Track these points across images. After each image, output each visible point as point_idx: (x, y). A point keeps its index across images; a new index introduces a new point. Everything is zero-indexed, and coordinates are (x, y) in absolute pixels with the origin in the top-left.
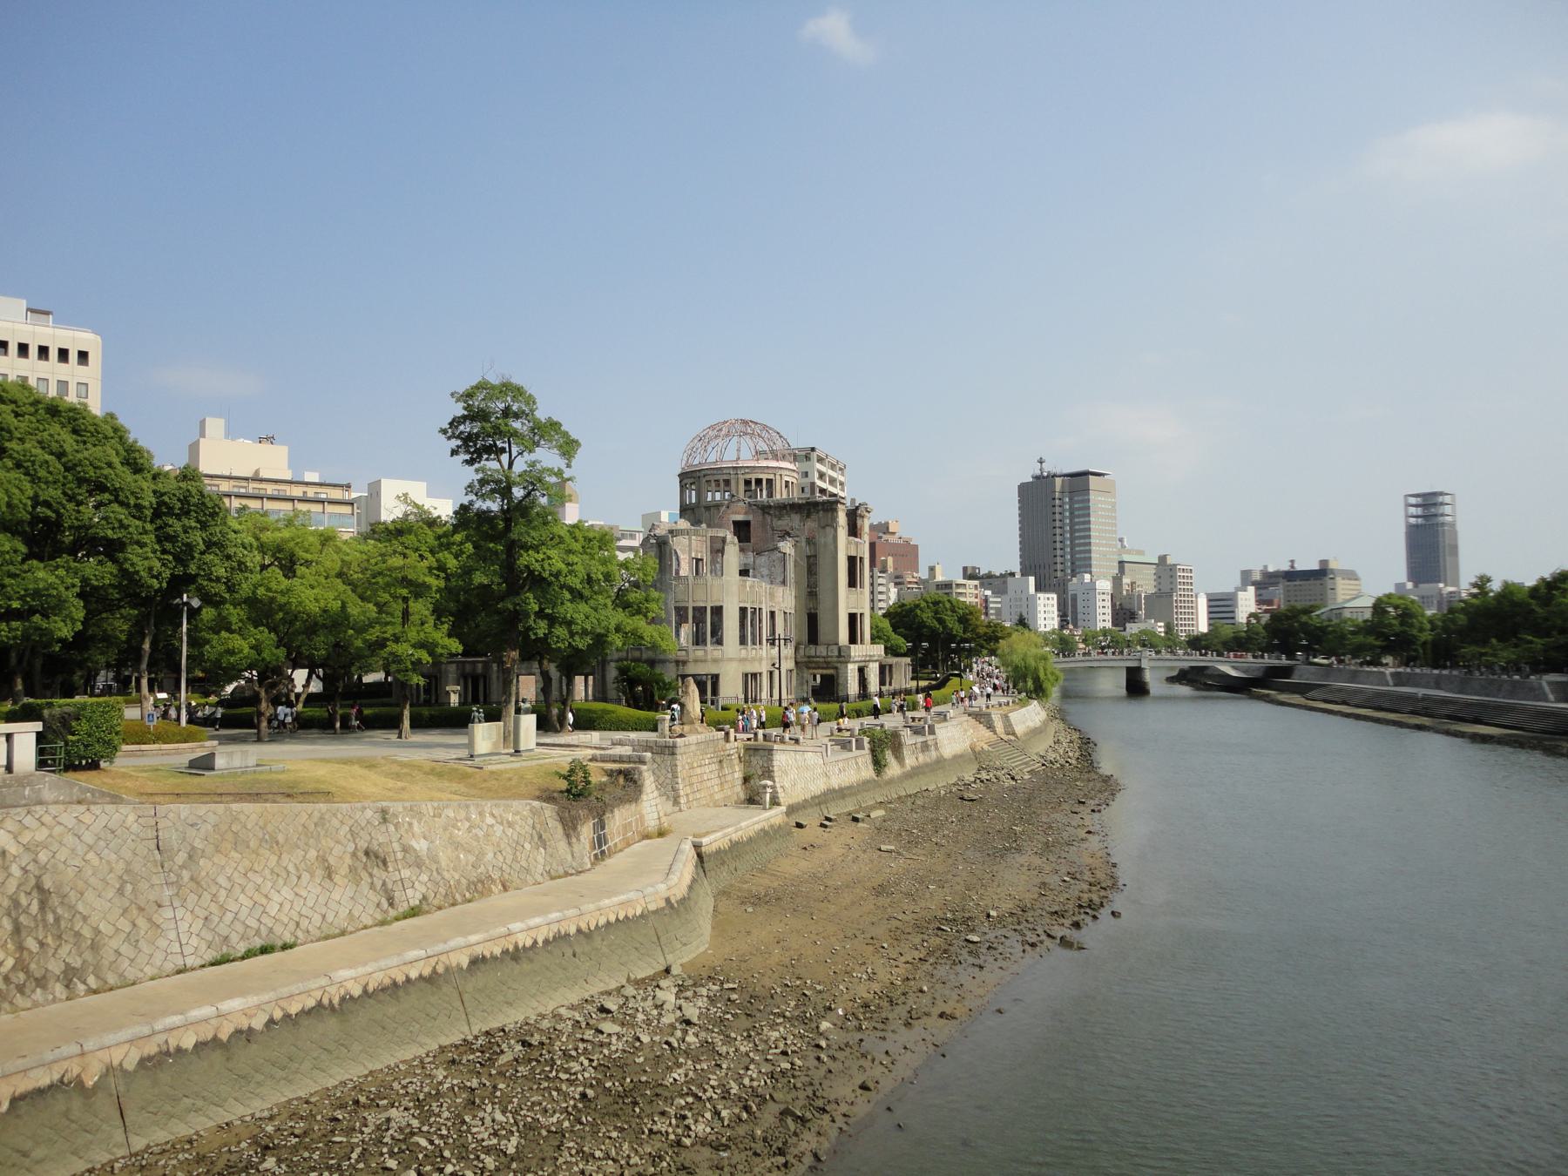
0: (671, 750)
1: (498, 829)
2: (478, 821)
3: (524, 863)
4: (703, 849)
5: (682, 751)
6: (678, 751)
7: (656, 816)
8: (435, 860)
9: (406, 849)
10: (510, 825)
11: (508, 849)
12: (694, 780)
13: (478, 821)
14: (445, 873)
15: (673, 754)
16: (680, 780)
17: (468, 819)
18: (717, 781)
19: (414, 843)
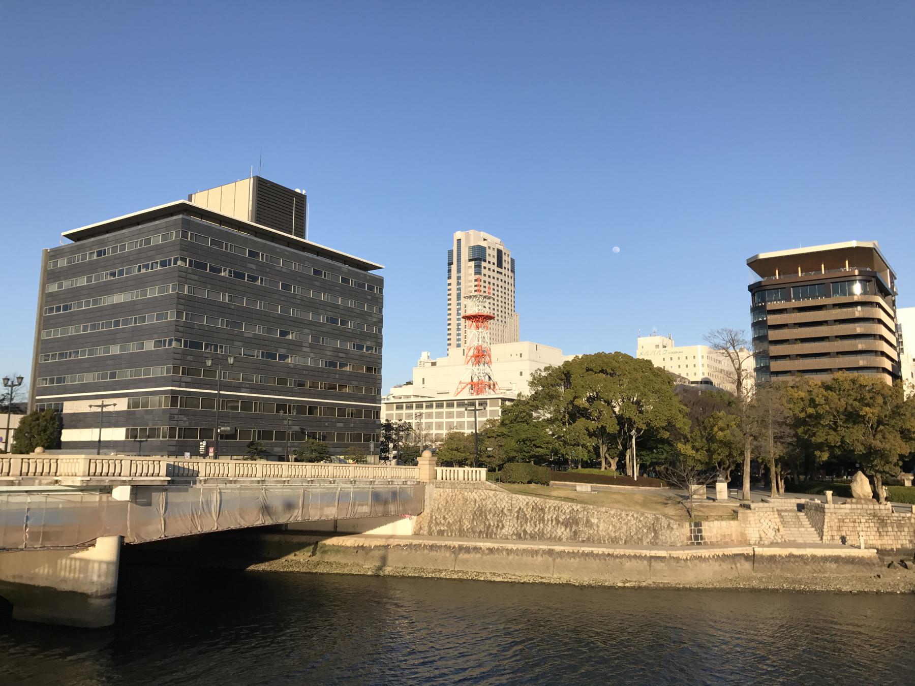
0: (821, 510)
1: (633, 522)
2: (625, 517)
3: (640, 536)
4: (756, 553)
5: (832, 511)
6: (826, 511)
7: (758, 536)
8: (598, 527)
9: (588, 521)
10: (640, 521)
11: (634, 530)
12: (845, 529)
13: (625, 517)
14: (600, 533)
15: (824, 512)
16: (825, 527)
17: (620, 515)
18: (874, 533)
19: (592, 520)
